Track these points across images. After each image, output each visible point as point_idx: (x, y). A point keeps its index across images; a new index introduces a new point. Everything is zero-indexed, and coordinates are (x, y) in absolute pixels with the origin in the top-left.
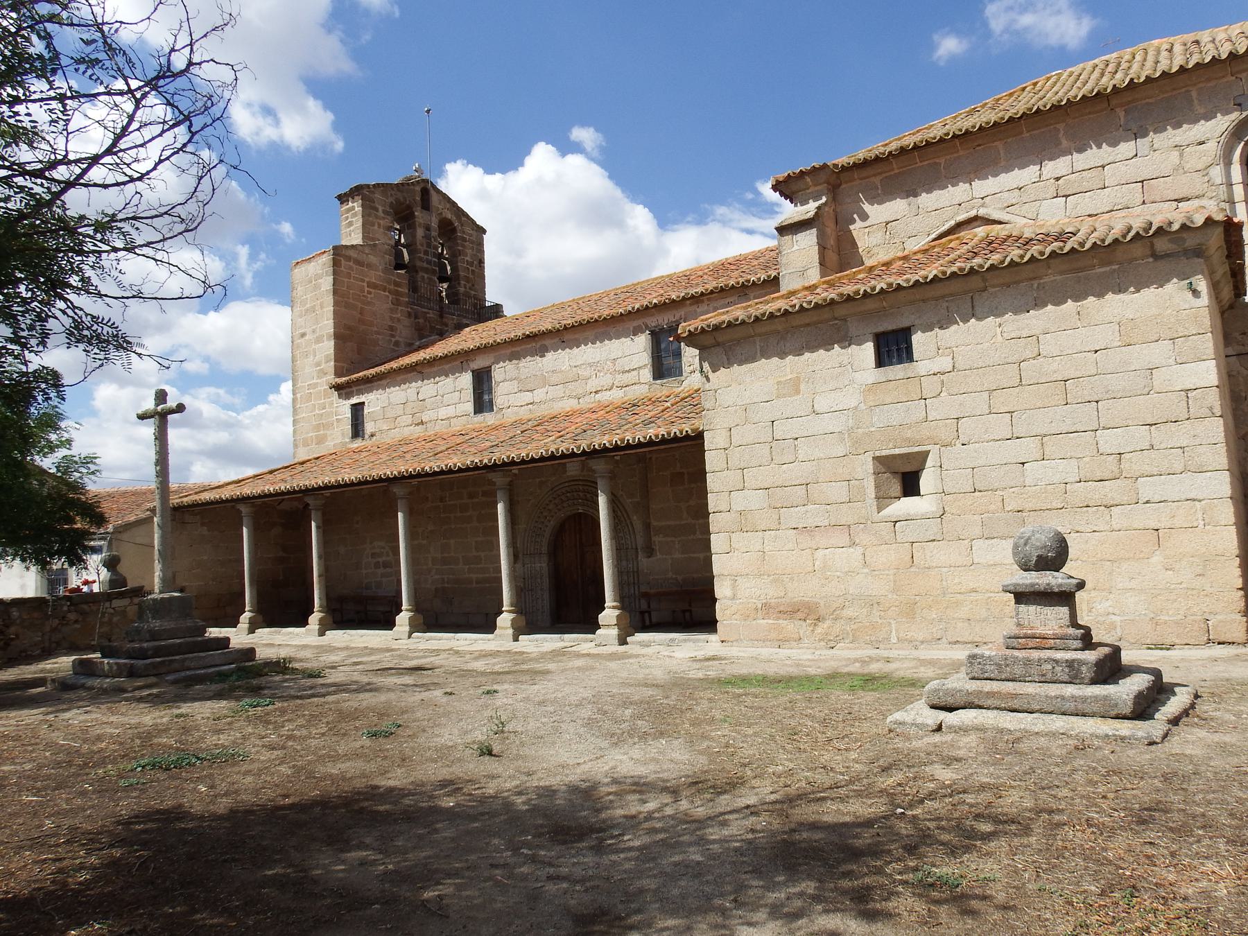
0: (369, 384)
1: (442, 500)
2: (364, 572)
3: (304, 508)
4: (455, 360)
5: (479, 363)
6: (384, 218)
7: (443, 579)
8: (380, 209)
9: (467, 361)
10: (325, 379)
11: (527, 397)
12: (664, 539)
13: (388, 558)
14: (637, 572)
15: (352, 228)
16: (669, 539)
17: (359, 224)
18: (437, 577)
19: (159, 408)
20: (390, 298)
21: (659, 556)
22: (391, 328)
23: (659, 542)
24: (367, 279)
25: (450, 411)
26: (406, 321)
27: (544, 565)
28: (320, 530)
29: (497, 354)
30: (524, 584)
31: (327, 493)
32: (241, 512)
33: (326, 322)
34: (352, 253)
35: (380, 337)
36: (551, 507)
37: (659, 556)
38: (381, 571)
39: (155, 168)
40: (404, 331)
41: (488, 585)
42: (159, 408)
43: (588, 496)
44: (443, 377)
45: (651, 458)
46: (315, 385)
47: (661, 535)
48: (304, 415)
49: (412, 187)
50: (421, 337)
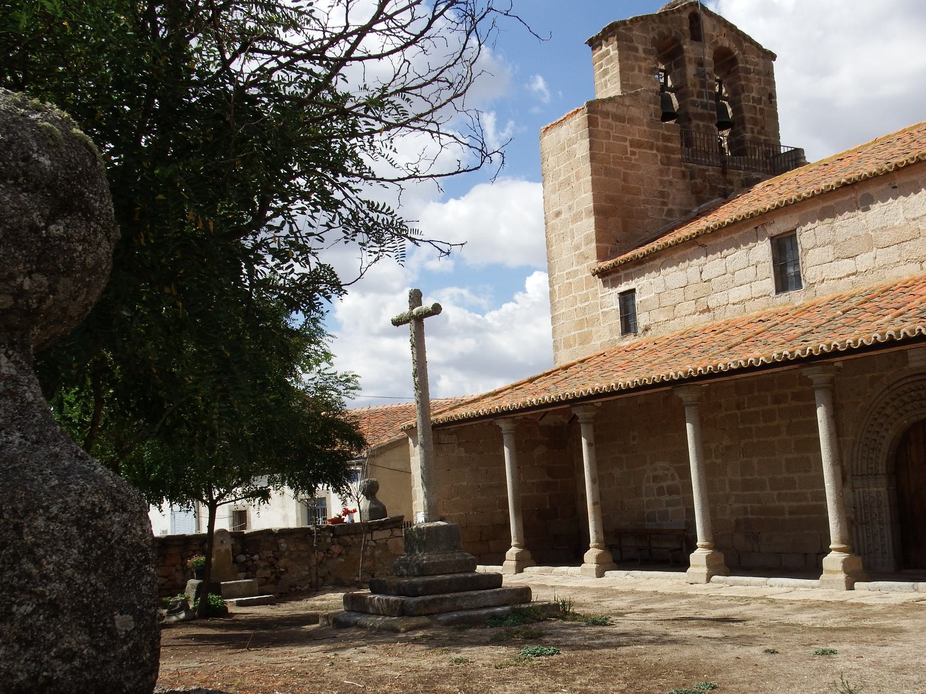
0: (639, 265)
1: (739, 406)
2: (645, 499)
3: (570, 422)
4: (747, 225)
5: (780, 226)
6: (646, 59)
7: (745, 508)
8: (641, 48)
9: (762, 225)
10: (586, 265)
11: (848, 266)
13: (674, 482)
15: (607, 77)
17: (616, 70)
18: (736, 505)
19: (415, 311)
20: (659, 157)
22: (662, 194)
24: (629, 138)
25: (743, 292)
26: (681, 184)
27: (882, 489)
28: (593, 447)
29: (803, 212)
31: (598, 402)
32: (501, 429)
33: (583, 196)
34: (610, 108)
35: (650, 207)
36: (888, 411)
38: (666, 498)
39: (429, 27)
40: (678, 196)
41: (804, 516)
42: (415, 311)
44: (732, 250)
46: (576, 273)
48: (563, 310)
49: (677, 15)
50: (700, 201)
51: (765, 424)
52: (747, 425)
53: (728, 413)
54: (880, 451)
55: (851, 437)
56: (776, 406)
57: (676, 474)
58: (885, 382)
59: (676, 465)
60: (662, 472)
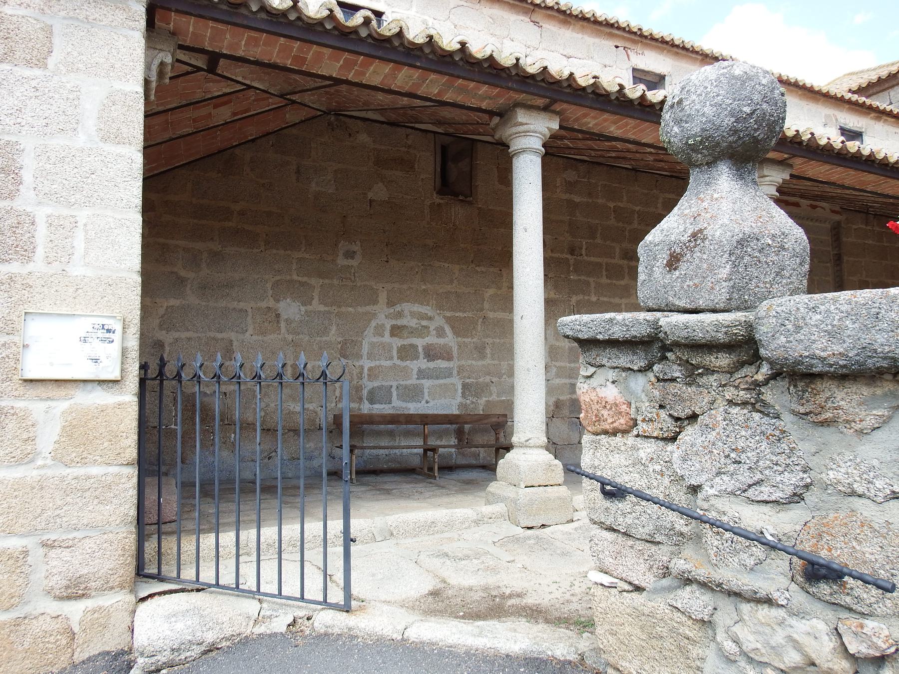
1: (572, 251)
2: (367, 364)
13: (441, 341)
51: (609, 281)
52: (583, 278)
53: (556, 255)
56: (626, 262)
57: (448, 329)
59: (448, 314)
60: (415, 321)
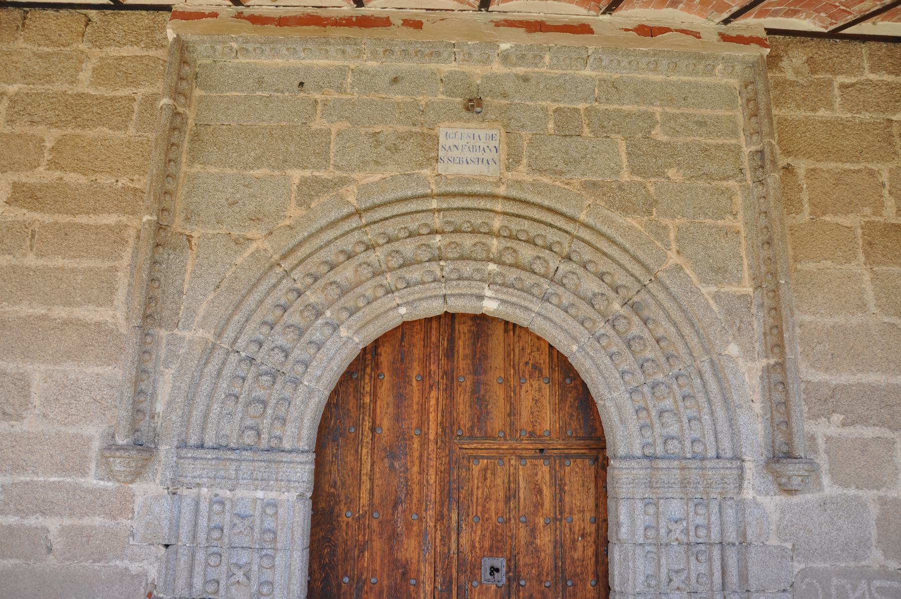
12: (846, 431)
14: (744, 543)
16: (869, 432)
21: (829, 488)
23: (829, 439)
30: (169, 568)
36: (346, 274)
37: (829, 488)
43: (526, 253)
45: (788, 169)
47: (837, 418)
54: (296, 382)
55: (200, 333)
58: (352, 199)
